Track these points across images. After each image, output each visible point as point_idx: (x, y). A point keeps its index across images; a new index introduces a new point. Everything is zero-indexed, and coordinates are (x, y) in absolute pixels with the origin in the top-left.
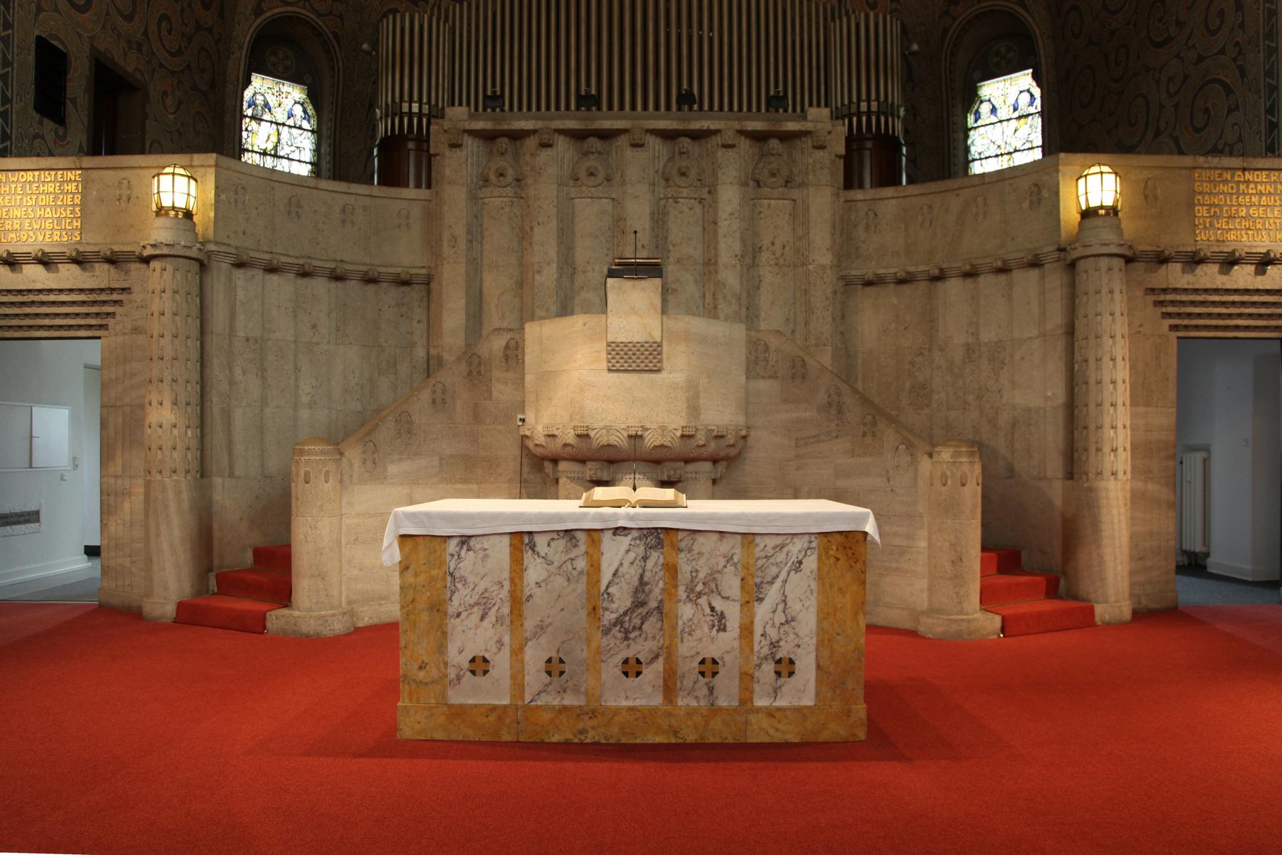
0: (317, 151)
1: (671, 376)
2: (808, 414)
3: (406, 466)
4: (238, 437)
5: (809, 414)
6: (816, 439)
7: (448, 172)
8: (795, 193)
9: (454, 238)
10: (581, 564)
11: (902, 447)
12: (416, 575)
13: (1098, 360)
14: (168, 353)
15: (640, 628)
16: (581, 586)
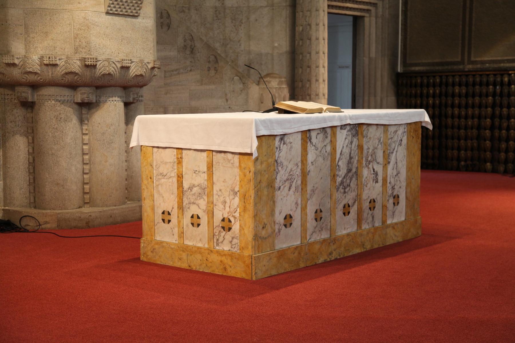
1: (144, 21)
2: (172, 54)
5: (173, 53)
6: (177, 72)
10: (329, 148)
11: (236, 78)
12: (262, 163)
13: (317, 25)
15: (349, 185)
16: (328, 163)
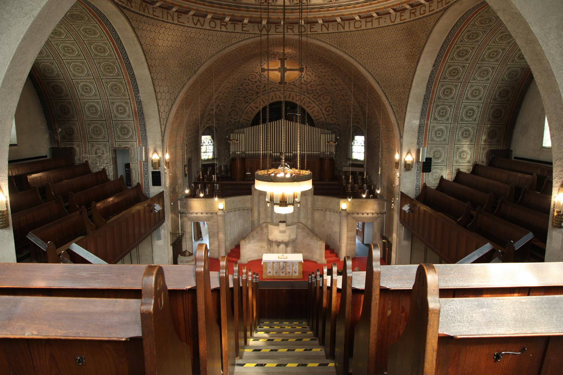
0: (214, 149)
3: (253, 241)
5: (305, 234)
7: (255, 194)
8: (306, 197)
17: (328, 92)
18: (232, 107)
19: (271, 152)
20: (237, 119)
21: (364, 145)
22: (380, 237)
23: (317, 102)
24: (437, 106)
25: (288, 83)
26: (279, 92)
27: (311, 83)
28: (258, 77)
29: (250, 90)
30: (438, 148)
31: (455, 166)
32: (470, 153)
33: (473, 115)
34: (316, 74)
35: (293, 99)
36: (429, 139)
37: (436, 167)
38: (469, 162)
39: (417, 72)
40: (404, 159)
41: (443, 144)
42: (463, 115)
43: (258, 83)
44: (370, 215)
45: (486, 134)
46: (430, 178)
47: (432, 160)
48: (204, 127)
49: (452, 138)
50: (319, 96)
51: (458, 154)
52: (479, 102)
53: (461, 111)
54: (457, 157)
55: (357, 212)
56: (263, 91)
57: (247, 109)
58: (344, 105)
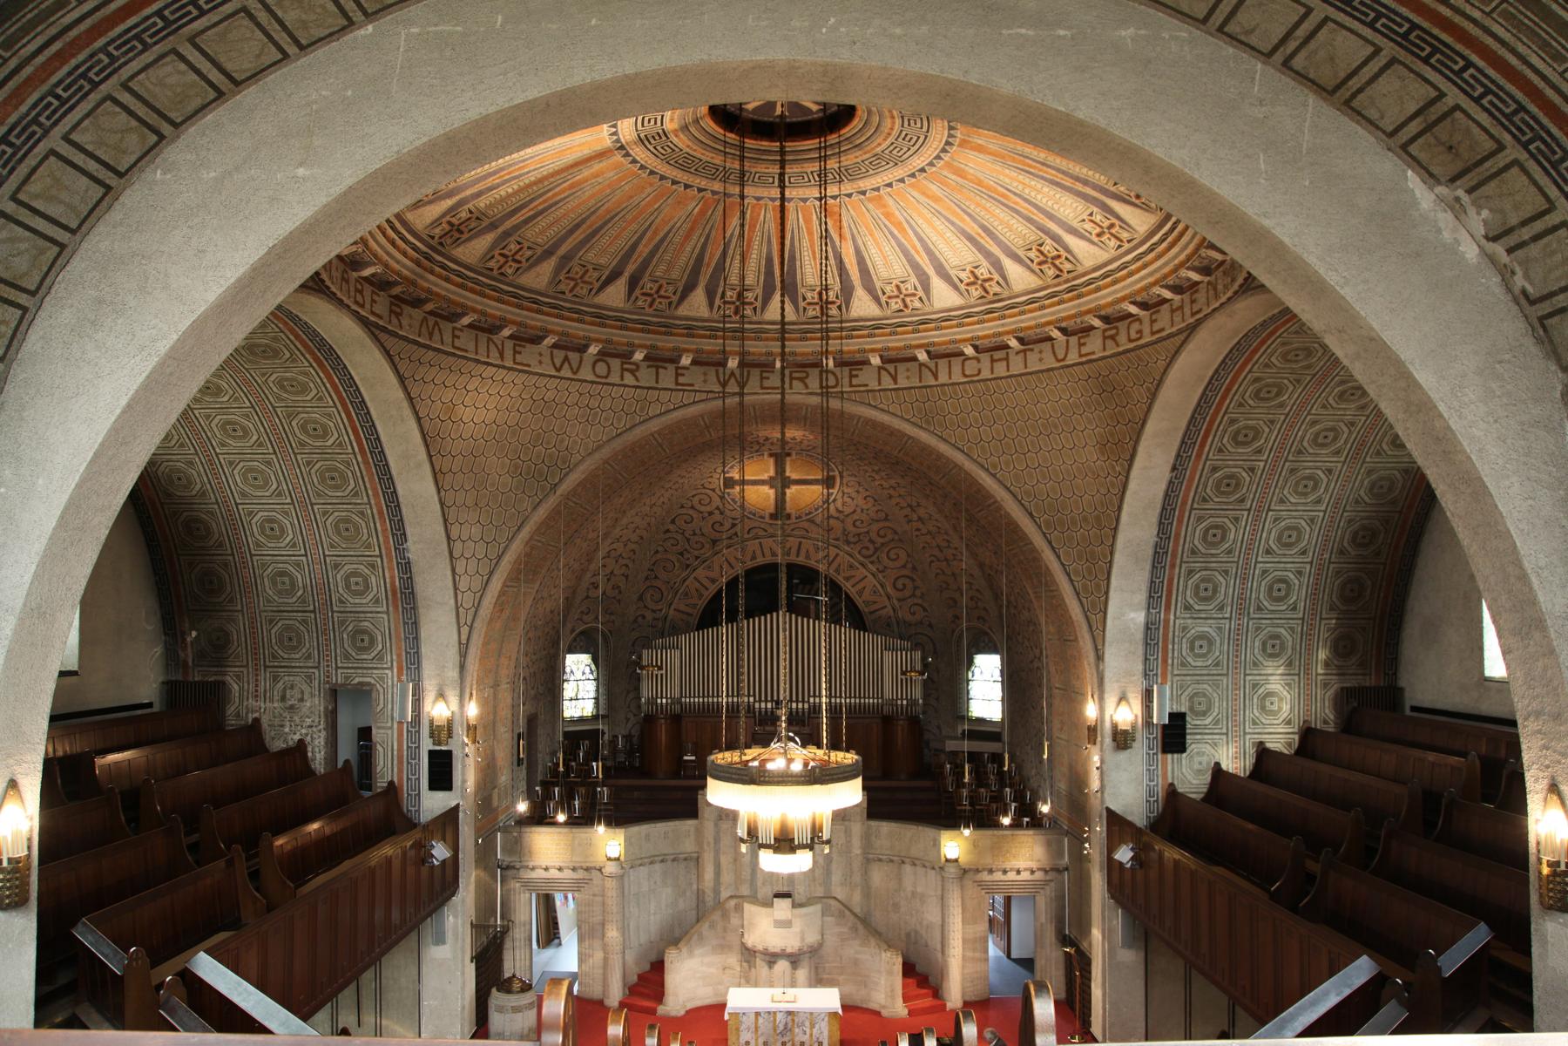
0: (597, 691)
4: (631, 933)
5: (846, 930)
8: (846, 823)
9: (709, 843)
14: (615, 911)
16: (771, 1024)
17: (900, 540)
18: (647, 578)
19: (752, 699)
20: (661, 610)
21: (1000, 679)
22: (1057, 938)
23: (870, 566)
24: (1190, 572)
25: (793, 516)
26: (771, 539)
27: (855, 517)
28: (717, 502)
29: (695, 534)
30: (1201, 686)
31: (1250, 733)
32: (1289, 696)
33: (1287, 595)
34: (868, 493)
35: (808, 557)
36: (1175, 661)
37: (1198, 737)
38: (1288, 722)
39: (1133, 485)
40: (1111, 716)
41: (1213, 675)
42: (1261, 597)
43: (717, 517)
44: (1025, 876)
45: (1329, 643)
46: (1184, 770)
47: (1188, 718)
48: (573, 631)
49: (1237, 656)
50: (876, 550)
51: (1255, 700)
52: (1300, 560)
53: (1255, 584)
54: (1255, 711)
55: (989, 867)
56: (730, 538)
57: (686, 584)
58: (944, 573)
